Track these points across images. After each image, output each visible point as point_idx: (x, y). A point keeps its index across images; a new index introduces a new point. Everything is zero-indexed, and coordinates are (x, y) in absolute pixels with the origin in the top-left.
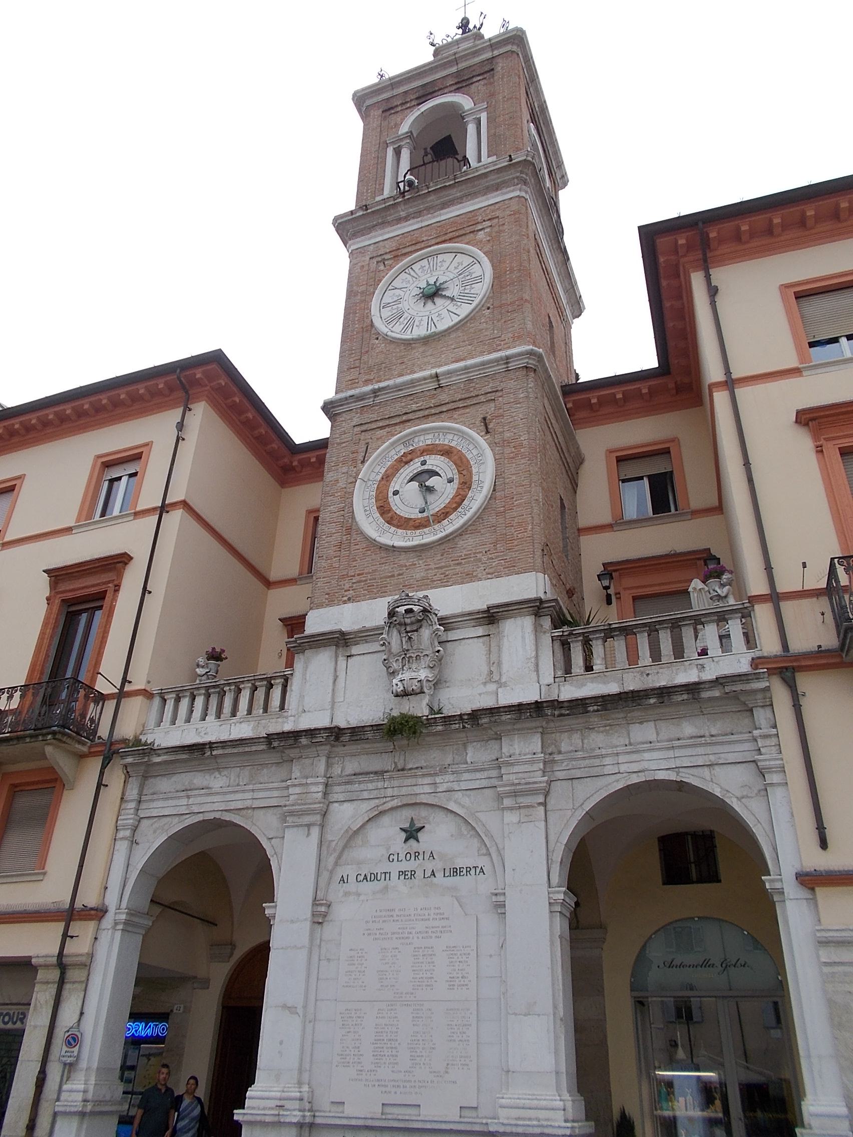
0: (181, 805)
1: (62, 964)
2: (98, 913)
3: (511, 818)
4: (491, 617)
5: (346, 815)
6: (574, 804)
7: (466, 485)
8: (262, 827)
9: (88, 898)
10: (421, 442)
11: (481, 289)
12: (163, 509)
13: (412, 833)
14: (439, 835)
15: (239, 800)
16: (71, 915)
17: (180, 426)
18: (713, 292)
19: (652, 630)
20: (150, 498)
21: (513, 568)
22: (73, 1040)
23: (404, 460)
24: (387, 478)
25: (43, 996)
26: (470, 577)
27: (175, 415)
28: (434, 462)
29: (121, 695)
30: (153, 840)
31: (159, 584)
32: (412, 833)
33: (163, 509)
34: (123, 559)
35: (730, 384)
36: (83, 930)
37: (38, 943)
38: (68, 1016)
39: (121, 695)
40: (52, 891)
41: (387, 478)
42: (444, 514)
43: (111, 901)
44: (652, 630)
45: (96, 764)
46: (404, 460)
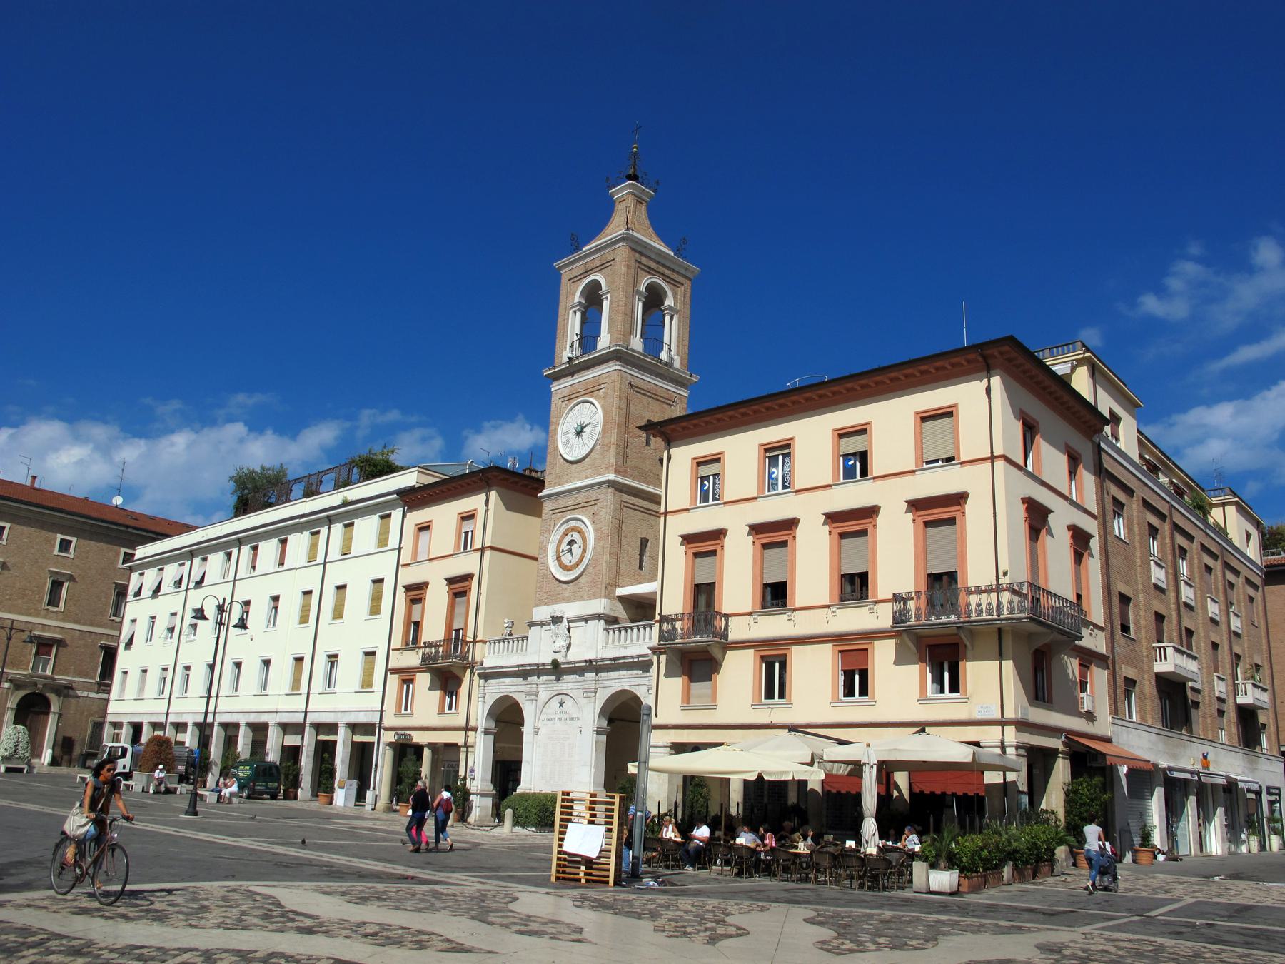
0: (495, 689)
1: (466, 745)
2: (475, 729)
4: (586, 619)
5: (543, 696)
7: (584, 551)
8: (520, 698)
9: (472, 724)
10: (572, 523)
11: (598, 430)
12: (483, 549)
13: (561, 704)
14: (569, 703)
15: (513, 689)
16: (467, 729)
17: (487, 503)
18: (669, 459)
20: (478, 545)
21: (594, 596)
22: (472, 771)
24: (560, 542)
25: (463, 756)
26: (582, 598)
27: (483, 497)
28: (576, 536)
29: (475, 642)
30: (490, 701)
31: (484, 590)
32: (561, 704)
33: (483, 549)
35: (666, 513)
36: (471, 734)
37: (458, 738)
39: (475, 642)
40: (461, 721)
41: (560, 542)
42: (577, 565)
43: (479, 724)
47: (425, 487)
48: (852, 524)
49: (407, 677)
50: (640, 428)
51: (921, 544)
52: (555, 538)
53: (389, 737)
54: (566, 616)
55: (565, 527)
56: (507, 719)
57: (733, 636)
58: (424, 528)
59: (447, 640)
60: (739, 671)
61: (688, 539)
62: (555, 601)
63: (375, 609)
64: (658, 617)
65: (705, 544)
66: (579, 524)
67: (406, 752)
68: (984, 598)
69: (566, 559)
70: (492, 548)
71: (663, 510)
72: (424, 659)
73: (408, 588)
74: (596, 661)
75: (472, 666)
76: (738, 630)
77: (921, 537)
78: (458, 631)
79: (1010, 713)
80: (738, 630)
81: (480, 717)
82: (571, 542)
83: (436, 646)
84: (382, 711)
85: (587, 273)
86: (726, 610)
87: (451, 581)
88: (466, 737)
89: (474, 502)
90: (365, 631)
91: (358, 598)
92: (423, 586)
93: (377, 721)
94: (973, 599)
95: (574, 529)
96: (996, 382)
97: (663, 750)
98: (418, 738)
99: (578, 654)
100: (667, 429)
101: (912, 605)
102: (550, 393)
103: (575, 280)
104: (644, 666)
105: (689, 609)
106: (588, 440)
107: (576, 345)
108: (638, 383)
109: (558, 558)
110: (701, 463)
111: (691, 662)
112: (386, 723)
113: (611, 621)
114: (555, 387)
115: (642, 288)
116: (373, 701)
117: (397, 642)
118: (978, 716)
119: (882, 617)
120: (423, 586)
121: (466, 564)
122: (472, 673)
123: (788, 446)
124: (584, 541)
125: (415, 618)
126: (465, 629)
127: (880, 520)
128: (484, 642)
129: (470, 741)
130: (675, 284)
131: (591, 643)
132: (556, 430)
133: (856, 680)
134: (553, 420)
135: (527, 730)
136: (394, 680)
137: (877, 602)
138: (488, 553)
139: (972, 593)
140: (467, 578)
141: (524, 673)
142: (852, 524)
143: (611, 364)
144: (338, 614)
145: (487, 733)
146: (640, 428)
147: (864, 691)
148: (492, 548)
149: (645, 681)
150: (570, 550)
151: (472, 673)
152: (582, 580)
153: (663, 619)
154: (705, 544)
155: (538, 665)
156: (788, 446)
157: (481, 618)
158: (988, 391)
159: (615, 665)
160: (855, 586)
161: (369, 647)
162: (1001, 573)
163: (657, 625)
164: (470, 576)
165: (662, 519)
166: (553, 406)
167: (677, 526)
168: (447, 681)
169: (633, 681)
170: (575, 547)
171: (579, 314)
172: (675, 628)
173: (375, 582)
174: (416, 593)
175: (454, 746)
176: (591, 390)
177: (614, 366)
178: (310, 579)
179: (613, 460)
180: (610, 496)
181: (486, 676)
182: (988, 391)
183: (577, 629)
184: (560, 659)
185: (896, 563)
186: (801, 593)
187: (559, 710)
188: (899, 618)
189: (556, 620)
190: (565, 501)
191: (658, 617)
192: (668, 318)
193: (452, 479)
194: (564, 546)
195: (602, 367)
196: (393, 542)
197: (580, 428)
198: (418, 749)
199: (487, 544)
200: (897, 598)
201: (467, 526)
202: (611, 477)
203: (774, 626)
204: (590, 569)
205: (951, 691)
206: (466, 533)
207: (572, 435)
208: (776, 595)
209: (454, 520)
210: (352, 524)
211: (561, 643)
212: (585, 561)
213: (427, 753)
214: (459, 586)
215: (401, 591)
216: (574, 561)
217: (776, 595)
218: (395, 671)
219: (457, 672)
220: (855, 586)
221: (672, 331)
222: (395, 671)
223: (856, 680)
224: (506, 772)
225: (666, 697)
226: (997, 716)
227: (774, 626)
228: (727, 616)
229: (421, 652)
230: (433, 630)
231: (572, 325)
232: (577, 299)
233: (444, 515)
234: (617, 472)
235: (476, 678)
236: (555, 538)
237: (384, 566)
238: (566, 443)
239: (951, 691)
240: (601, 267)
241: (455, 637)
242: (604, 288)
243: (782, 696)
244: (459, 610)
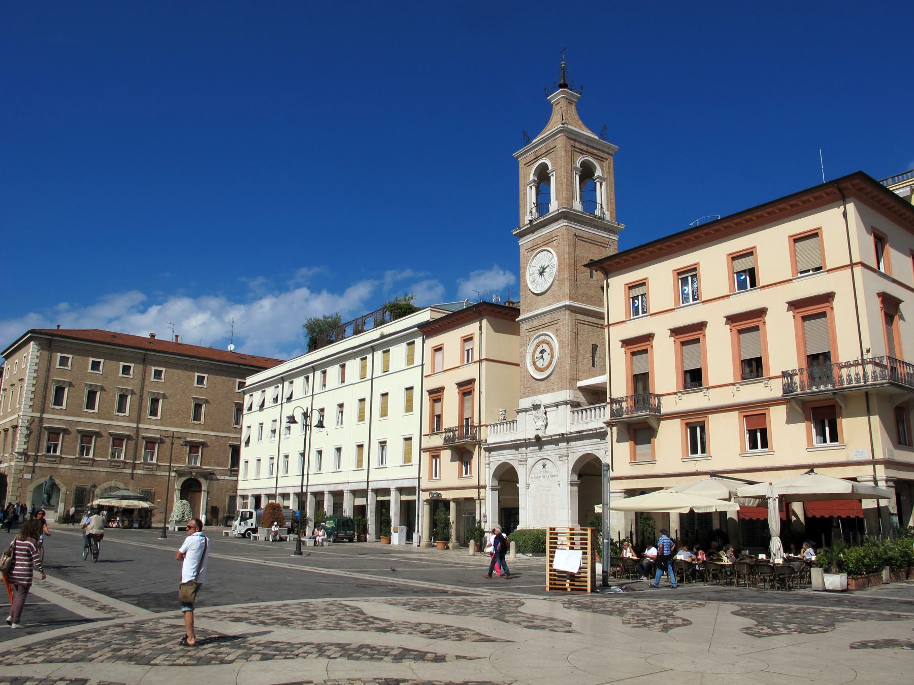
1: (479, 498)
2: (485, 487)
3: (561, 463)
4: (557, 405)
5: (531, 461)
6: (573, 459)
7: (552, 357)
8: (514, 464)
9: (482, 483)
11: (555, 270)
13: (544, 466)
14: (549, 465)
15: (509, 457)
16: (479, 487)
17: (480, 328)
18: (608, 286)
19: (590, 410)
20: (476, 358)
21: (562, 388)
22: (485, 516)
23: (538, 346)
24: (534, 352)
25: (477, 506)
26: (553, 391)
27: (477, 324)
28: (545, 347)
29: (480, 426)
30: (494, 467)
32: (544, 466)
33: (480, 361)
34: (472, 381)
35: (609, 325)
37: (473, 494)
38: (483, 511)
39: (480, 426)
40: (474, 482)
41: (534, 352)
42: (548, 367)
44: (590, 410)
45: (477, 447)
46: (538, 346)
47: (436, 321)
48: (747, 322)
49: (435, 453)
50: (585, 266)
51: (800, 333)
52: (530, 349)
53: (425, 496)
54: (542, 404)
55: (537, 341)
56: (507, 479)
57: (664, 410)
58: (439, 349)
59: (461, 426)
60: (671, 436)
61: (626, 343)
62: (534, 394)
63: (409, 408)
64: (608, 400)
65: (639, 345)
66: (547, 338)
67: (438, 505)
68: (853, 370)
69: (540, 364)
70: (487, 360)
71: (606, 323)
72: (446, 440)
73: (431, 392)
74: (567, 434)
75: (479, 443)
76: (667, 406)
77: (800, 328)
78: (467, 419)
79: (879, 455)
80: (667, 406)
81: (487, 478)
82: (543, 351)
83: (453, 431)
84: (419, 478)
85: (537, 158)
86: (657, 392)
87: (460, 385)
88: (479, 493)
89: (471, 328)
90: (403, 424)
91: (397, 401)
92: (441, 390)
93: (417, 485)
94: (844, 372)
95: (544, 342)
96: (851, 207)
97: (619, 495)
98: (446, 495)
99: (554, 430)
100: (605, 265)
101: (797, 379)
102: (518, 247)
103: (529, 164)
104: (602, 435)
105: (631, 393)
106: (549, 278)
107: (534, 210)
108: (581, 234)
109: (534, 363)
110: (631, 287)
111: (635, 430)
112: (423, 486)
113: (575, 405)
114: (522, 242)
115: (578, 165)
116: (412, 472)
117: (426, 430)
118: (854, 458)
119: (775, 389)
120: (441, 390)
121: (469, 372)
122: (480, 448)
123: (695, 269)
124: (552, 350)
125: (437, 412)
126: (472, 418)
127: (768, 318)
128: (487, 426)
129: (482, 495)
130: (601, 159)
131: (562, 421)
132: (525, 272)
133: (758, 437)
134: (522, 265)
135: (521, 485)
136: (426, 456)
137: (770, 378)
138: (484, 363)
139: (843, 367)
140: (471, 382)
141: (516, 446)
142: (747, 322)
143: (560, 222)
144: (384, 413)
145: (493, 489)
146: (585, 266)
147: (765, 445)
148: (487, 360)
149: (602, 446)
150: (542, 357)
151: (480, 448)
152: (552, 377)
153: (613, 401)
154: (639, 345)
155: (525, 440)
156: (695, 269)
157: (483, 409)
158: (845, 215)
159: (580, 436)
160: (753, 368)
161: (407, 434)
162: (864, 351)
163: (609, 406)
164: (473, 381)
165: (606, 330)
166: (521, 256)
167: (618, 334)
168: (463, 455)
169: (594, 447)
170: (545, 355)
171: (534, 188)
172: (621, 408)
173: (407, 389)
174: (436, 395)
175: (471, 500)
176: (548, 242)
177: (562, 223)
178: (363, 390)
179: (567, 291)
180: (567, 317)
181: (489, 450)
182: (845, 215)
183: (551, 413)
184: (541, 434)
185: (783, 348)
186: (712, 376)
187: (542, 470)
188: (788, 389)
189: (536, 407)
190: (536, 323)
191: (608, 400)
192: (598, 185)
193: (454, 313)
194: (538, 355)
195: (553, 225)
196: (418, 360)
197: (542, 270)
198: (446, 503)
199: (483, 357)
200: (785, 374)
201: (468, 346)
202: (567, 302)
203: (694, 401)
204: (557, 369)
205: (831, 441)
206: (468, 351)
207: (536, 275)
208: (694, 378)
209: (458, 342)
210: (388, 351)
211: (541, 423)
212: (554, 364)
213: (452, 505)
214: (466, 388)
215: (426, 394)
216: (545, 365)
217: (694, 378)
218: (426, 450)
219: (469, 448)
220: (753, 368)
221: (602, 194)
222: (426, 450)
223: (758, 437)
224: (509, 515)
225: (619, 456)
226: (868, 457)
227: (694, 401)
228: (659, 396)
229: (443, 435)
230: (451, 420)
231: (530, 196)
232: (532, 178)
233: (451, 339)
234: (571, 299)
235: (483, 451)
236: (530, 349)
237: (413, 378)
238: (533, 281)
239: (831, 441)
240: (547, 153)
241: (466, 424)
242: (550, 168)
243: (703, 451)
244: (467, 404)
